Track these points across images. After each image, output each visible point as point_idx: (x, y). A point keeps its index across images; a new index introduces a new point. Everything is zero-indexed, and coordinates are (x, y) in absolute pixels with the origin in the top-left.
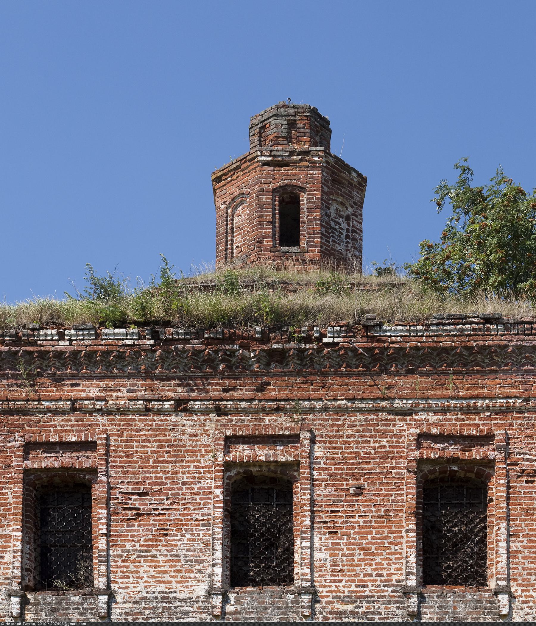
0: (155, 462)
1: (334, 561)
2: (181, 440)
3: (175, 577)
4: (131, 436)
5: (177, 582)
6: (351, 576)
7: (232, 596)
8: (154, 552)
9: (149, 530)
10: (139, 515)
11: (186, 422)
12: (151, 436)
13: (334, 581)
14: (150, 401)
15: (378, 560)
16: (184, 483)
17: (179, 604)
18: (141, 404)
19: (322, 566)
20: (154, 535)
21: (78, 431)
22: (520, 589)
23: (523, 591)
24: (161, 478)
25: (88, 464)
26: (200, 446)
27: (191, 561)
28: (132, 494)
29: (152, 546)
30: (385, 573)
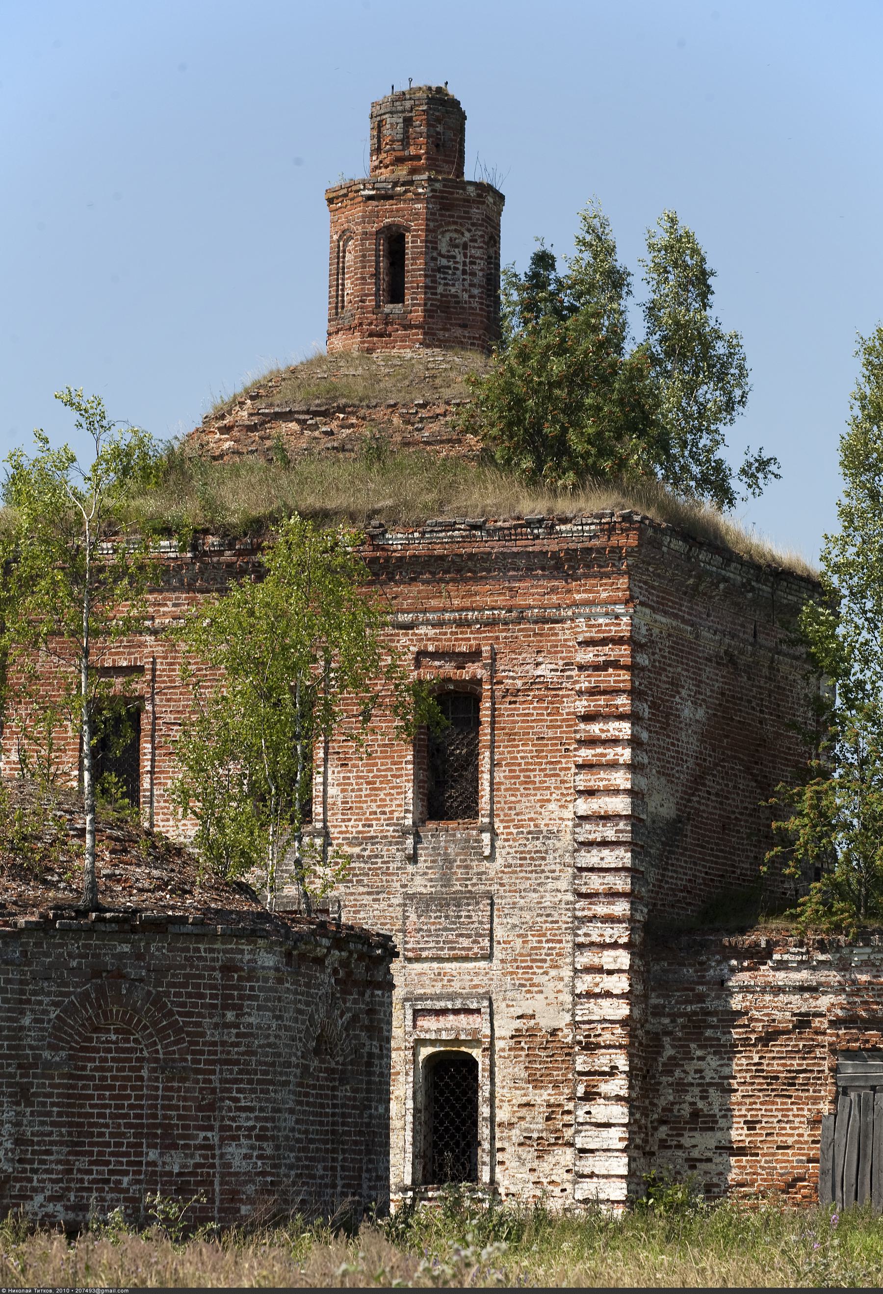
1: (344, 797)
6: (358, 814)
13: (343, 821)
15: (382, 796)
19: (334, 804)
22: (502, 825)
23: (505, 827)
30: (387, 810)
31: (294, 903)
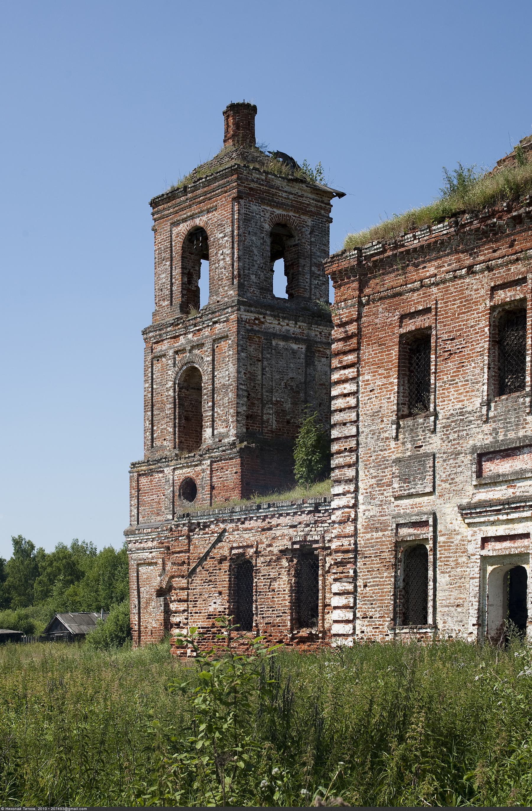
0: (458, 315)
2: (471, 295)
3: (466, 396)
4: (447, 298)
5: (467, 400)
7: (493, 405)
8: (457, 380)
9: (455, 365)
10: (451, 354)
11: (473, 281)
12: (456, 296)
14: (455, 271)
16: (472, 327)
17: (467, 415)
18: (451, 275)
20: (458, 368)
21: (424, 301)
24: (461, 325)
25: (427, 325)
26: (480, 297)
27: (474, 383)
28: (448, 340)
29: (456, 376)
31: (513, 443)
